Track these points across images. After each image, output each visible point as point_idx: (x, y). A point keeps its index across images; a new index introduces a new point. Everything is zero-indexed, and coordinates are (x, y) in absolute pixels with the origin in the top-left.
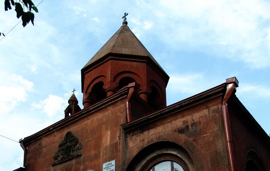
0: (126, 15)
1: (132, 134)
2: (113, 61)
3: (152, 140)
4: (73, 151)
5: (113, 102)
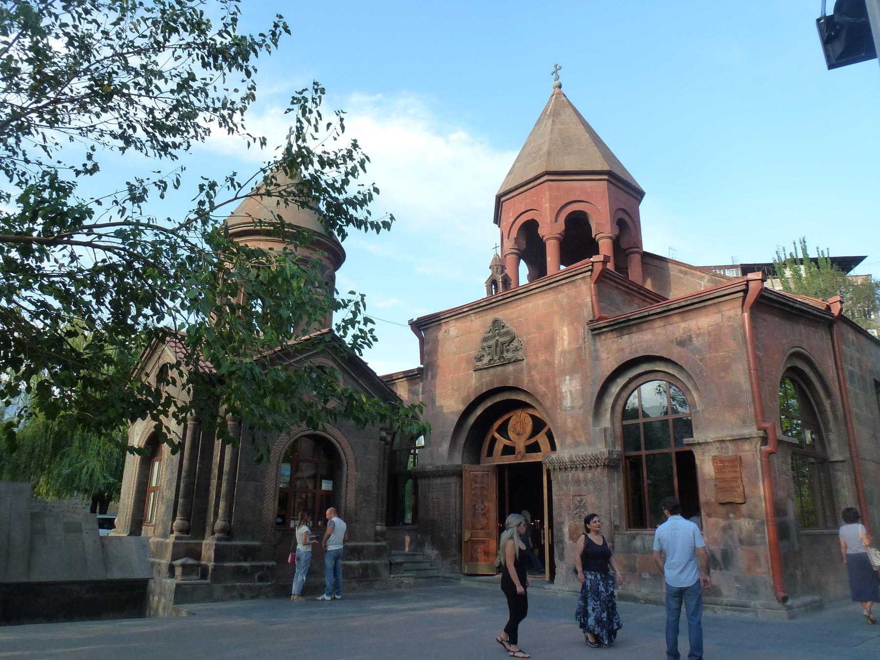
0: (557, 68)
1: (603, 337)
2: (550, 183)
3: (636, 351)
4: (508, 351)
5: (567, 280)
